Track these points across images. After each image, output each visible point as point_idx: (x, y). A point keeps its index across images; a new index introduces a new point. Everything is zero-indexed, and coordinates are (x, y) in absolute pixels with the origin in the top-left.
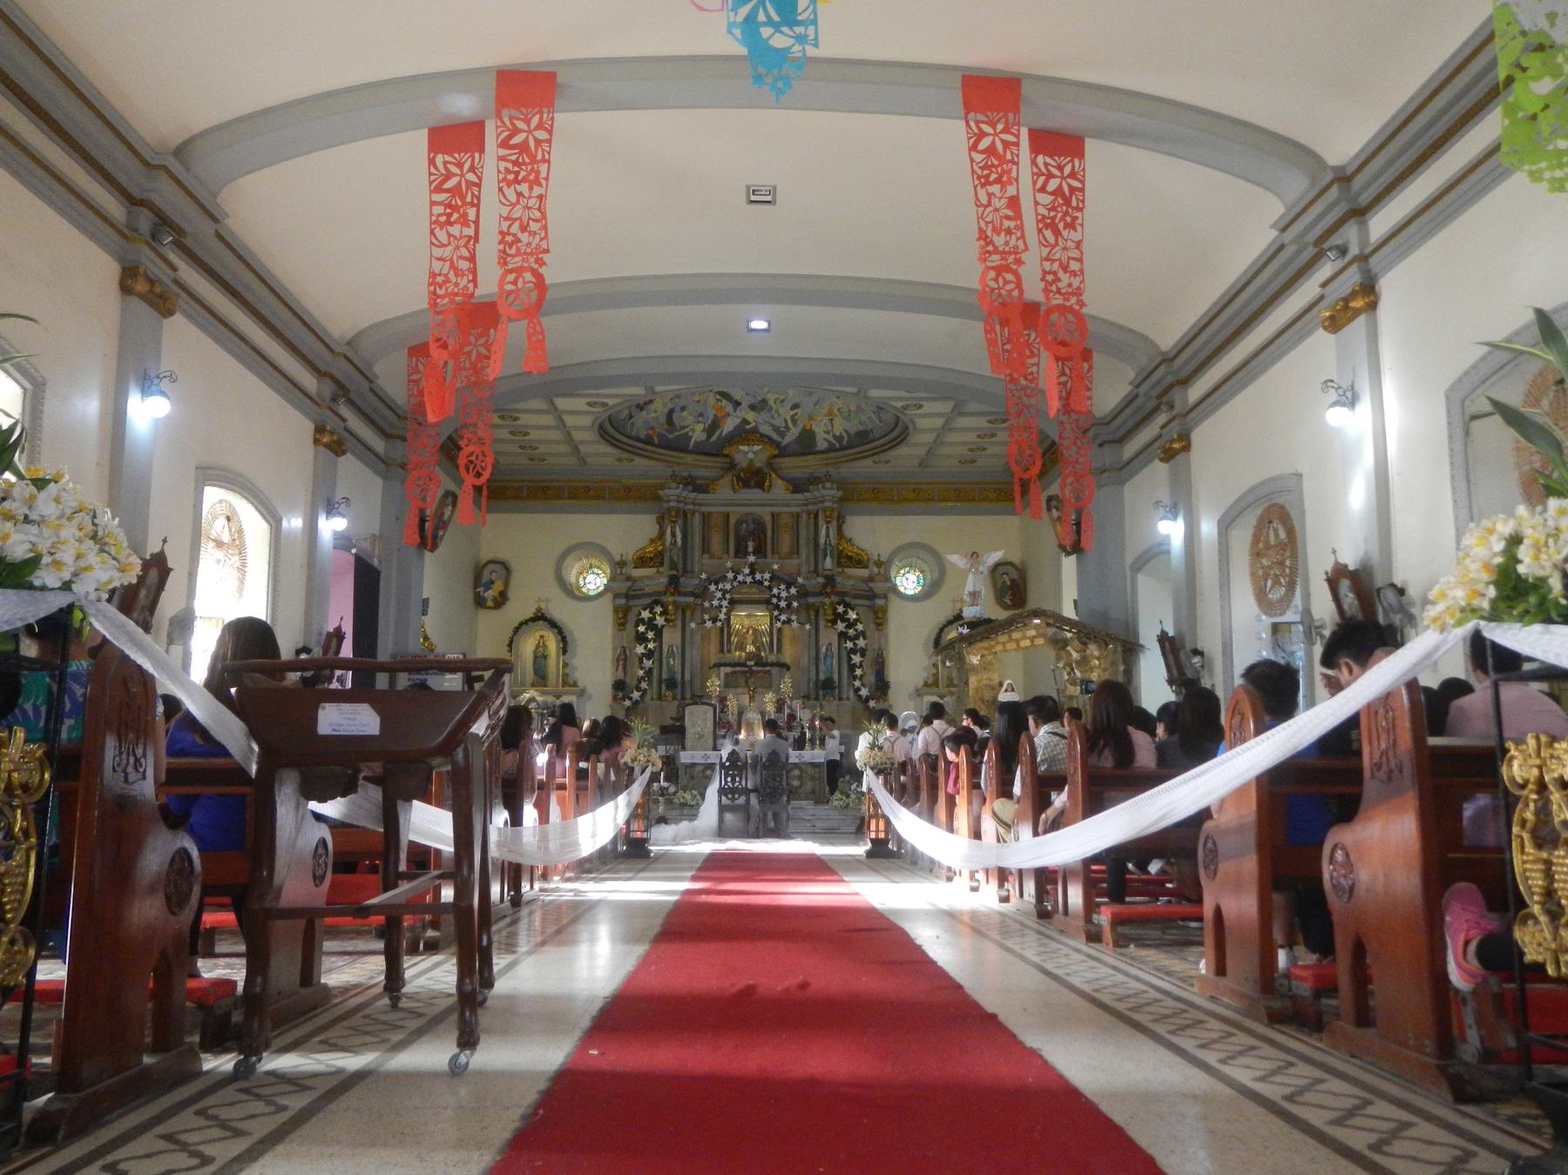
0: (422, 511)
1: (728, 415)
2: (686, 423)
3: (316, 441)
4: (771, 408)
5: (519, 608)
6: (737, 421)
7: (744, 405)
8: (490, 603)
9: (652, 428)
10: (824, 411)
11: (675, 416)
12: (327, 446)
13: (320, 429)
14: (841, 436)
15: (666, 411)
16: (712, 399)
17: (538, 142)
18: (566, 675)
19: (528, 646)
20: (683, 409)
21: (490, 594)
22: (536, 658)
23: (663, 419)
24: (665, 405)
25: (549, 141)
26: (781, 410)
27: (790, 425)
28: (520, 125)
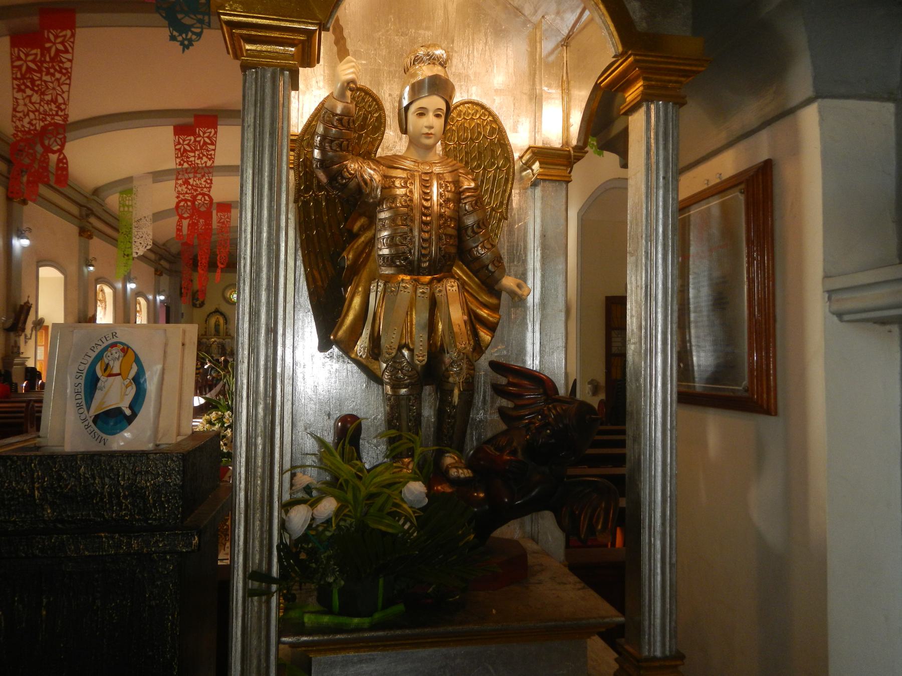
0: (181, 285)
3: (155, 274)
5: (209, 307)
8: (198, 306)
12: (159, 275)
13: (156, 270)
17: (227, 221)
18: (227, 332)
19: (213, 321)
21: (198, 303)
22: (215, 326)
25: (230, 222)
28: (223, 217)
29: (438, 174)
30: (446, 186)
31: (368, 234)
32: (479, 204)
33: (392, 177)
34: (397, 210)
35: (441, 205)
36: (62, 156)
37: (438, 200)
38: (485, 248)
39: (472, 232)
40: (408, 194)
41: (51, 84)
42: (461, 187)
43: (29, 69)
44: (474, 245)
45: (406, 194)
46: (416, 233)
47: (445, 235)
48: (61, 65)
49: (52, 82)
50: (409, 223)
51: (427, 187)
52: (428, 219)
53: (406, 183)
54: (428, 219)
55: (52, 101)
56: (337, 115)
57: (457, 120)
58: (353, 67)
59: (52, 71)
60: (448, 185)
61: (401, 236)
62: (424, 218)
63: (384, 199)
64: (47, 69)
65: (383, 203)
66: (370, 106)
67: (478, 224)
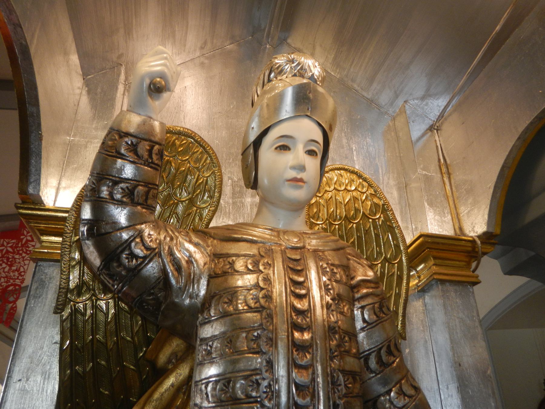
29: (315, 251)
30: (334, 274)
31: (183, 371)
32: (384, 309)
33: (228, 256)
34: (239, 319)
35: (328, 306)
36: (15, 306)
37: (321, 297)
38: (405, 395)
39: (377, 363)
40: (261, 284)
41: (18, 260)
42: (352, 278)
43: (8, 252)
44: (383, 390)
45: (257, 286)
46: (281, 371)
47: (343, 371)
48: (27, 249)
49: (19, 259)
50: (264, 348)
51: (298, 272)
52: (307, 336)
53: (256, 264)
54: (307, 336)
55: (16, 270)
56: (127, 134)
57: (326, 191)
58: (166, 58)
59: (21, 252)
60: (335, 271)
61: (246, 378)
62: (297, 335)
63: (213, 297)
64: (18, 251)
65: (210, 306)
66: (198, 160)
67: (389, 347)
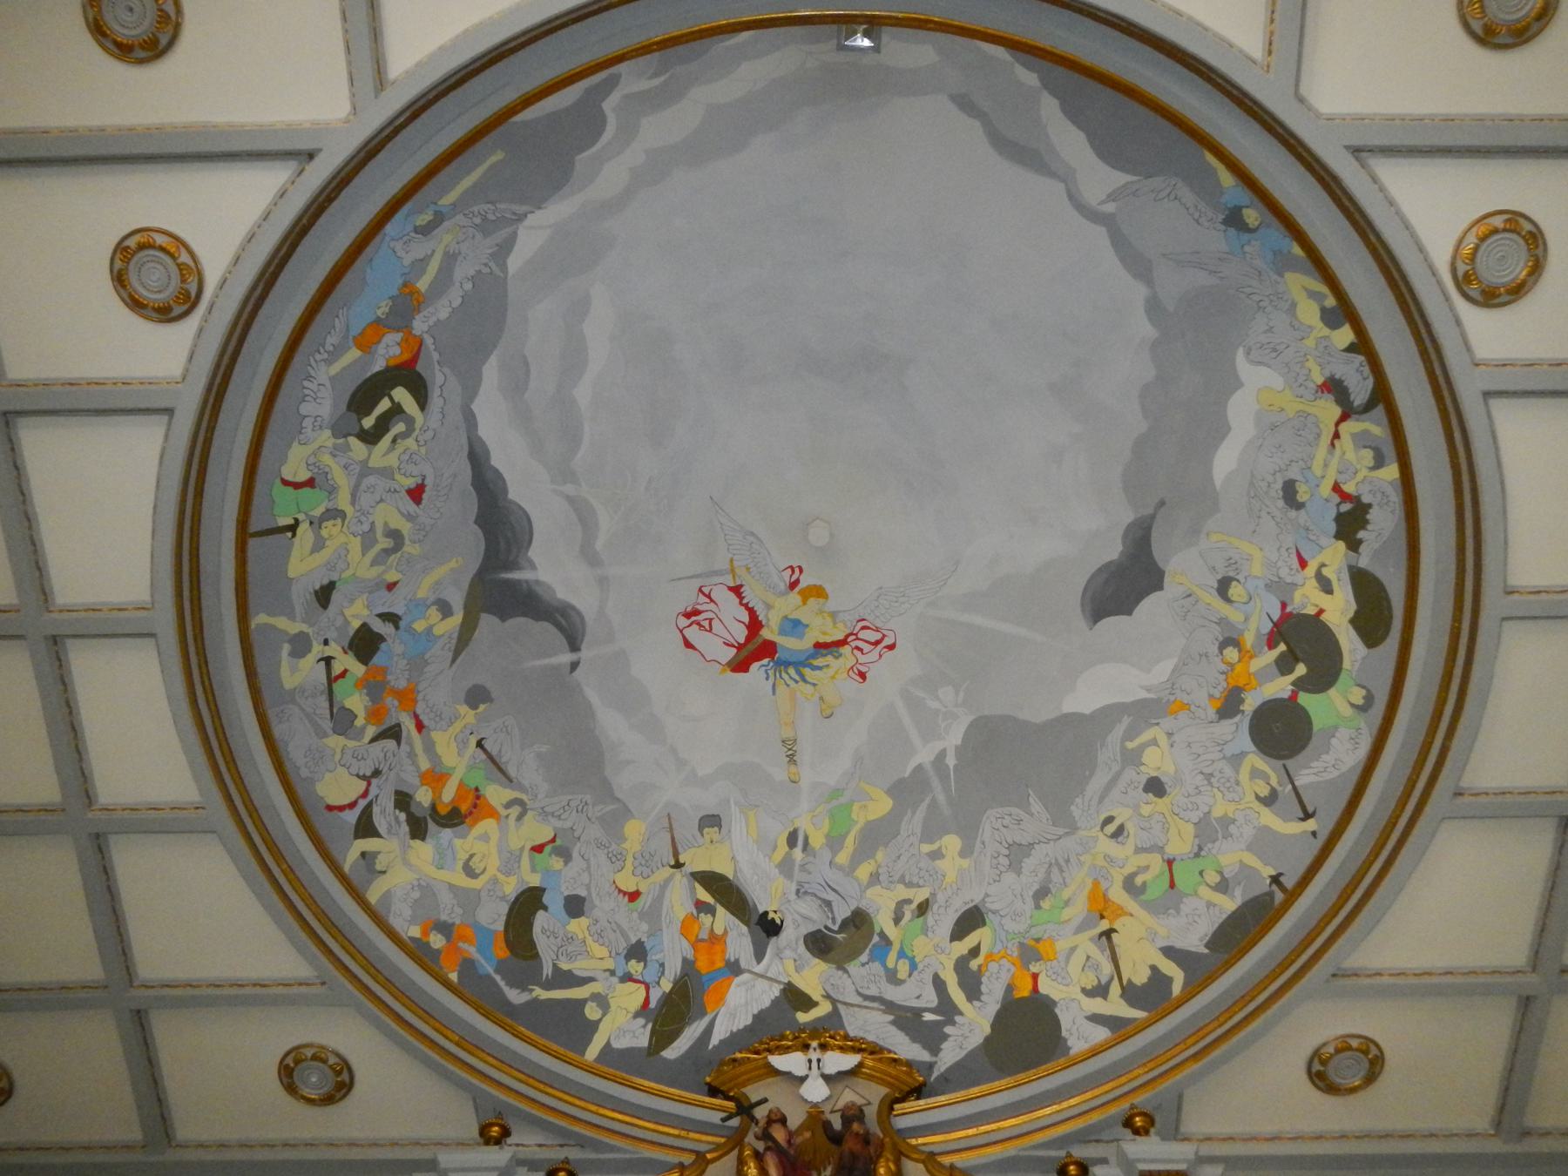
1: (735, 968)
2: (579, 967)
4: (886, 941)
6: (766, 995)
7: (792, 935)
9: (445, 928)
10: (1078, 910)
11: (540, 919)
14: (1158, 979)
15: (511, 888)
16: (680, 898)
20: (575, 906)
23: (494, 916)
24: (510, 864)
26: (921, 947)
27: (957, 995)
